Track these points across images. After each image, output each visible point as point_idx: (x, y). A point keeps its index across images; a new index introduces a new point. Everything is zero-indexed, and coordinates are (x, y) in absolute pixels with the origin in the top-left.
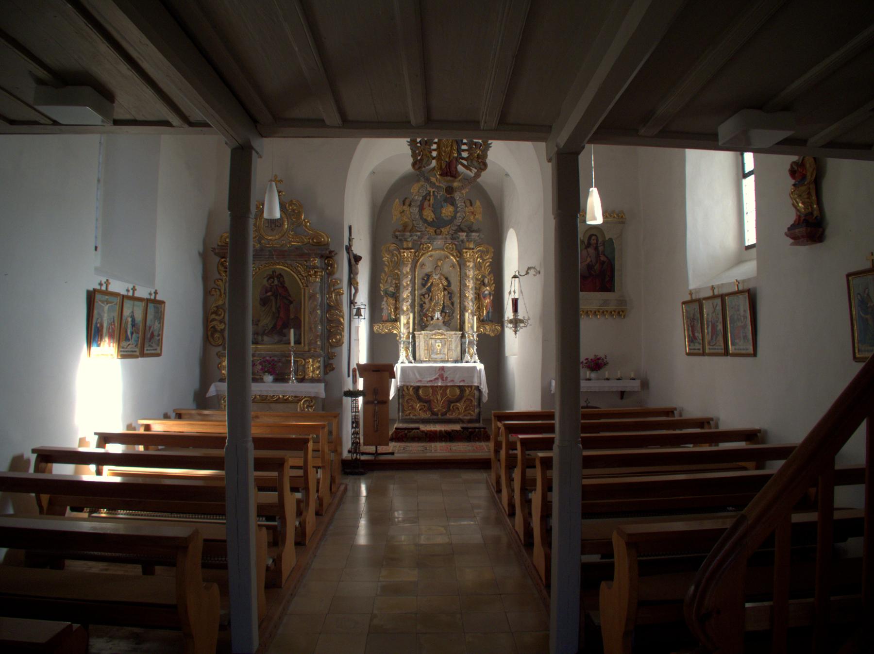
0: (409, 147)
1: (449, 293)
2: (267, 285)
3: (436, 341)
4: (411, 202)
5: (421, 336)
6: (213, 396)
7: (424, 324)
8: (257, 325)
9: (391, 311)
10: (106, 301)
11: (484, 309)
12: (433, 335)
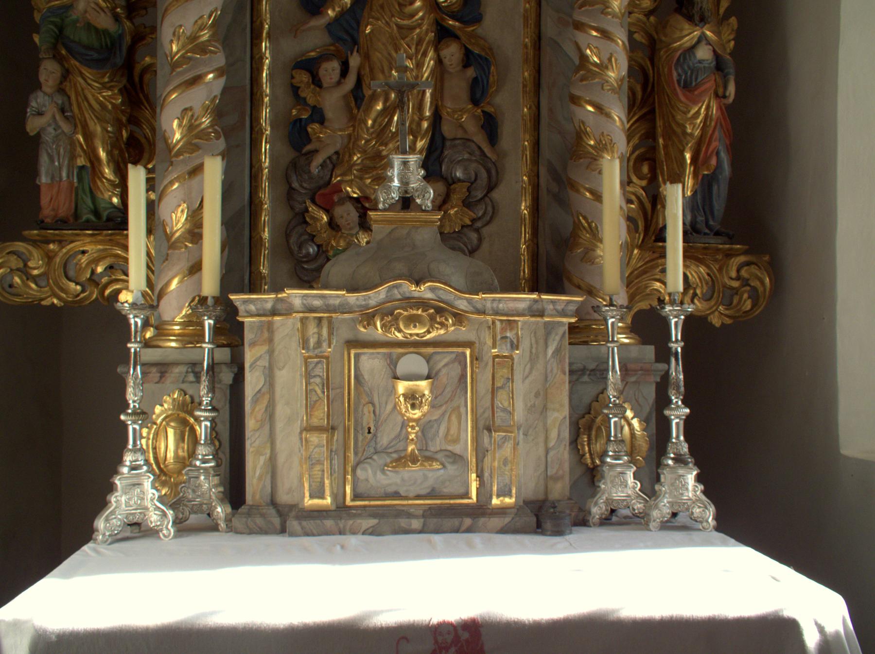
1: (468, 59)
3: (393, 363)
5: (285, 326)
7: (312, 250)
11: (688, 156)
12: (368, 318)
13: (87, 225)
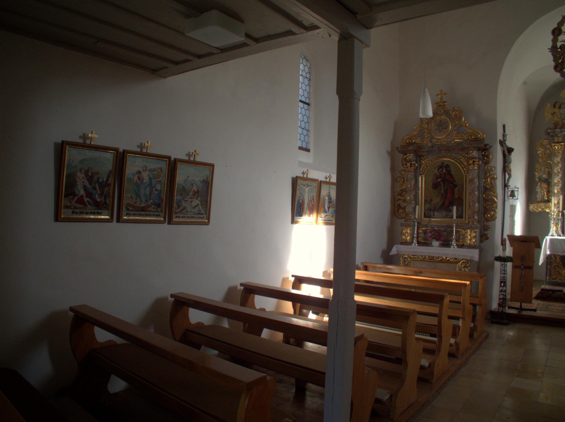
0: (551, 53)
2: (438, 174)
4: (560, 105)
6: (395, 254)
8: (430, 203)
9: (544, 193)
10: (307, 185)
13: (543, 202)
